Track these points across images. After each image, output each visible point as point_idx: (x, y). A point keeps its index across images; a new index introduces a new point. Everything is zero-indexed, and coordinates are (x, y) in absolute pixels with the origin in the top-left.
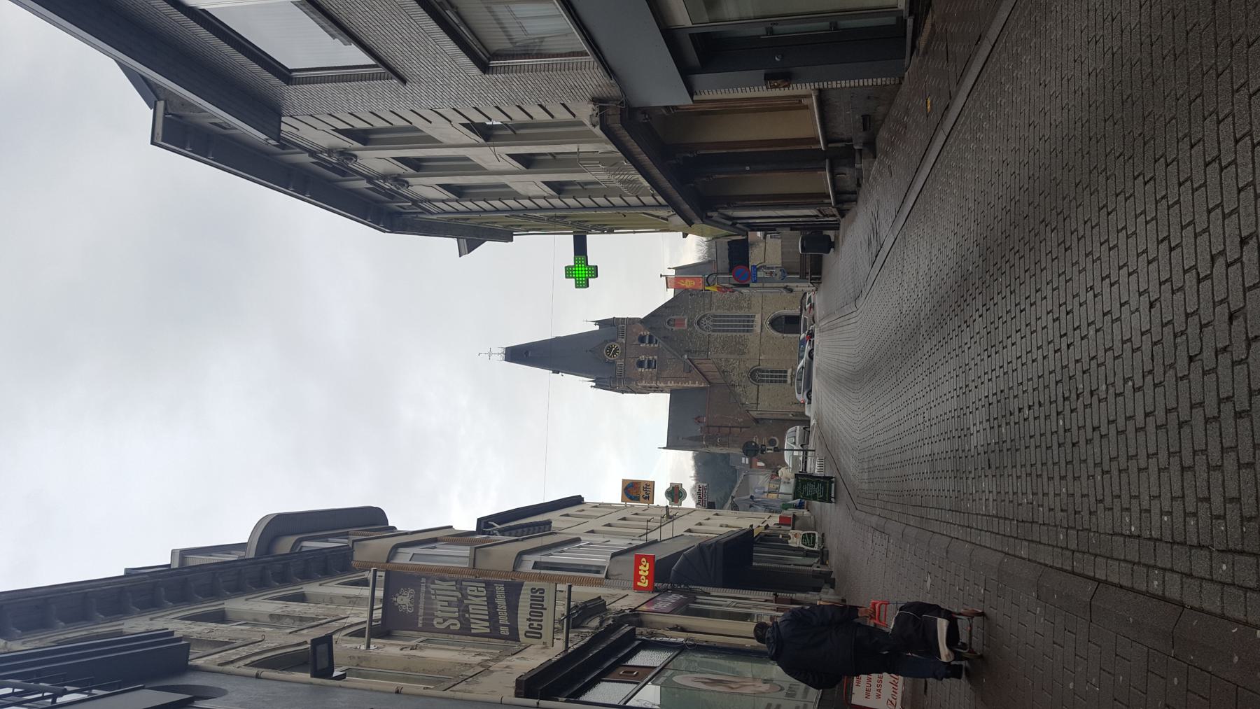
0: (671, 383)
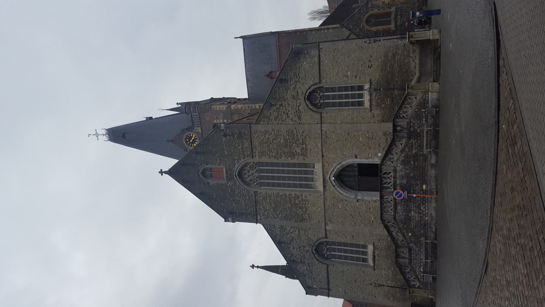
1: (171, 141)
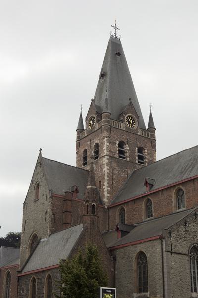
0: (108, 169)
1: (131, 103)
